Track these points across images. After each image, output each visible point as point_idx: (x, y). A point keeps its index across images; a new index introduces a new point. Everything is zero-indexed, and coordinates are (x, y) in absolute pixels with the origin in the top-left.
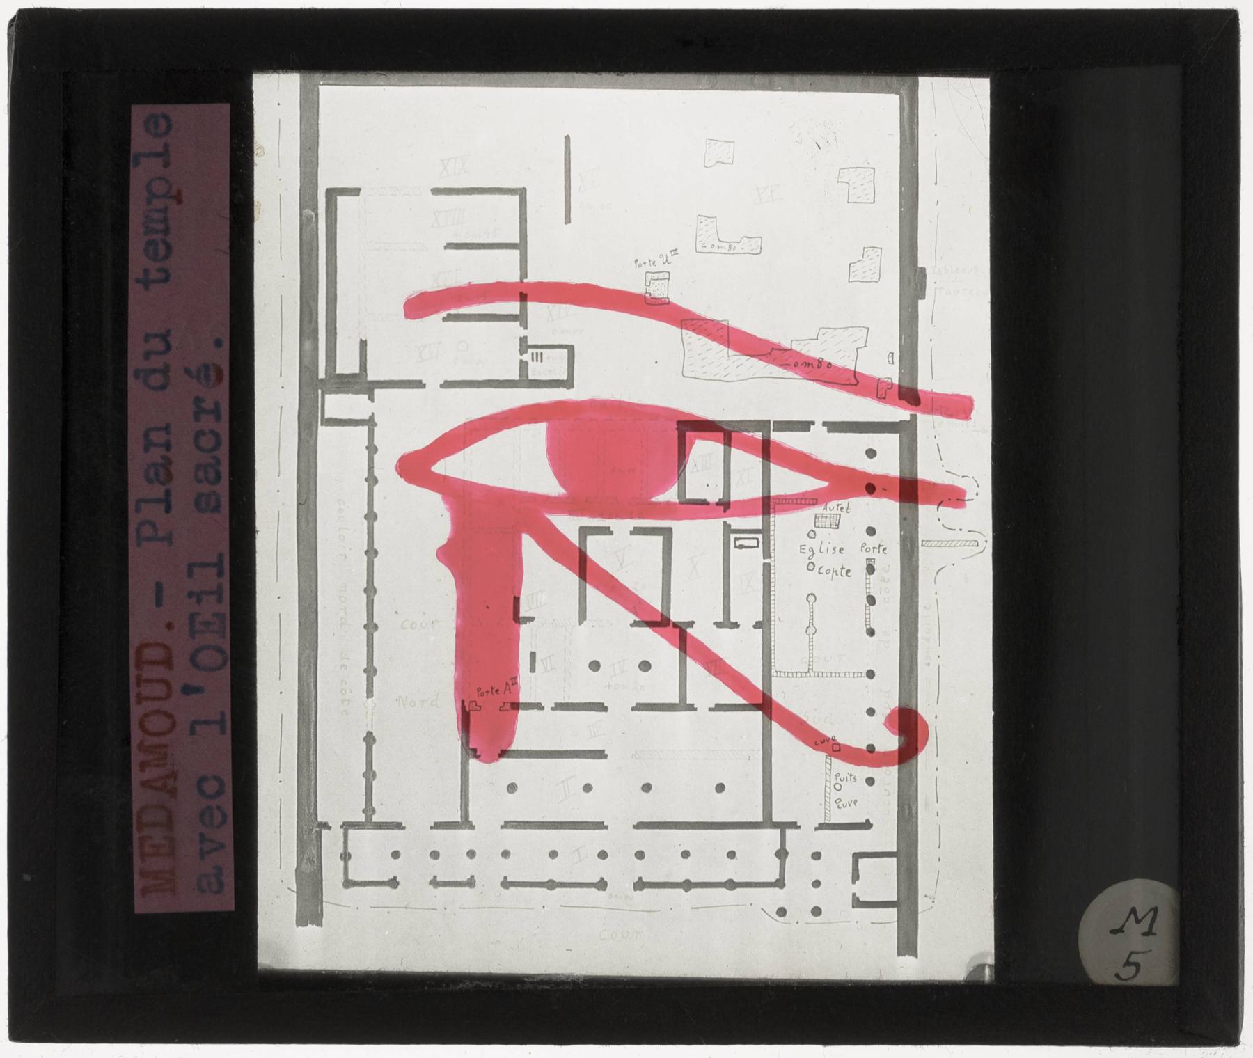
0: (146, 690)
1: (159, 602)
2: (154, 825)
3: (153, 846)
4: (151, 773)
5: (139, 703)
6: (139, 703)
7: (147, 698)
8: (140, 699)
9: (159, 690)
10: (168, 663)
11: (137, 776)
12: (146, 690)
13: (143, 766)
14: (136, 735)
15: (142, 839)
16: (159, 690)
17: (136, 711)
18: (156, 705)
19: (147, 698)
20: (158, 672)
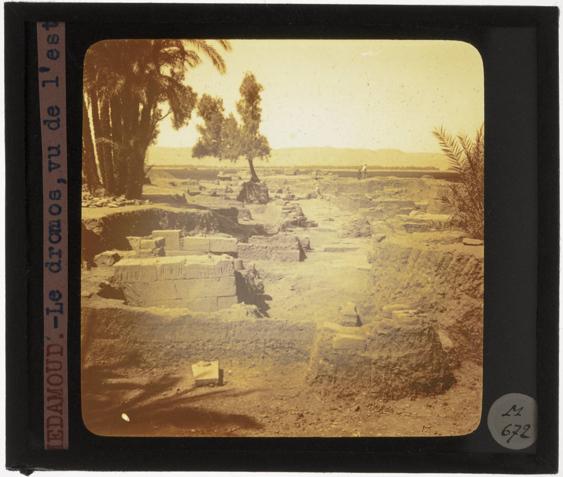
0: (51, 366)
1: (56, 326)
3: (52, 435)
4: (53, 402)
5: (47, 371)
6: (47, 371)
7: (51, 370)
8: (48, 370)
9: (57, 366)
11: (46, 404)
12: (51, 366)
13: (49, 399)
14: (46, 386)
15: (49, 432)
17: (46, 375)
18: (55, 372)
19: (51, 370)
20: (57, 357)
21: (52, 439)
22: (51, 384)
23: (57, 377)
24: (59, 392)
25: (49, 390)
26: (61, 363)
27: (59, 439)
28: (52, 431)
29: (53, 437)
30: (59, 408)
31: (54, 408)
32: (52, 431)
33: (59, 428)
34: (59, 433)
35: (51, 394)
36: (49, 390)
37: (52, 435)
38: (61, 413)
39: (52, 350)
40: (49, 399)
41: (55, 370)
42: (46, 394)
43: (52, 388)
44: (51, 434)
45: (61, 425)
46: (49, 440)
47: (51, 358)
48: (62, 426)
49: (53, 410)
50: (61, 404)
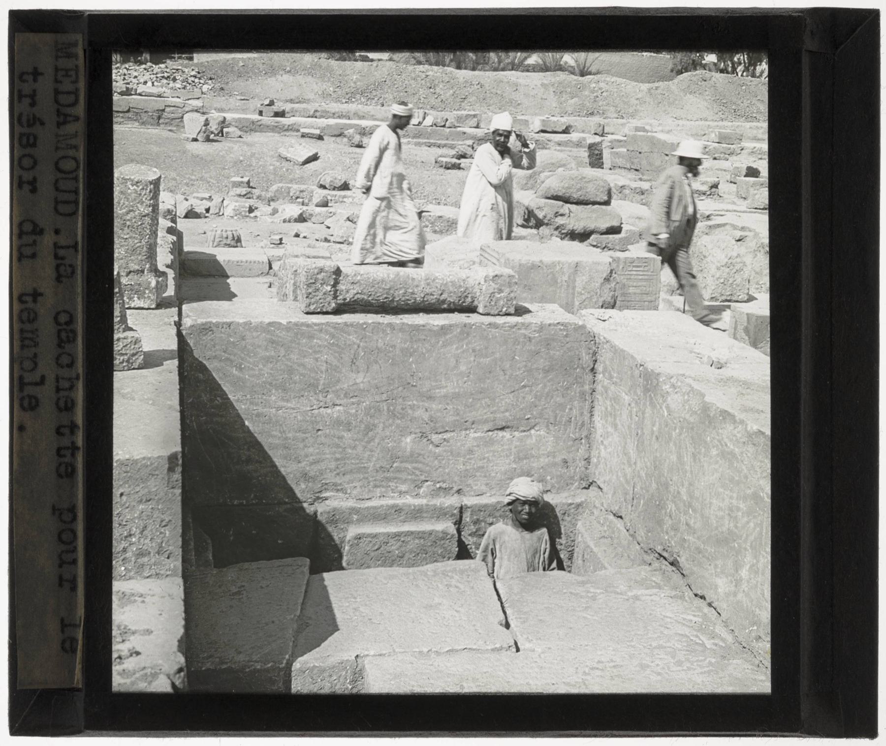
2: (69, 93)
3: (71, 76)
7: (73, 179)
13: (76, 135)
15: (76, 82)
18: (67, 176)
19: (73, 179)
25: (76, 147)
26: (57, 189)
27: (62, 70)
28: (73, 82)
30: (62, 119)
31: (69, 119)
32: (73, 82)
34: (59, 78)
36: (76, 147)
37: (71, 76)
38: (58, 111)
41: (66, 179)
43: (71, 153)
45: (57, 92)
47: (72, 197)
49: (70, 116)
50: (59, 125)
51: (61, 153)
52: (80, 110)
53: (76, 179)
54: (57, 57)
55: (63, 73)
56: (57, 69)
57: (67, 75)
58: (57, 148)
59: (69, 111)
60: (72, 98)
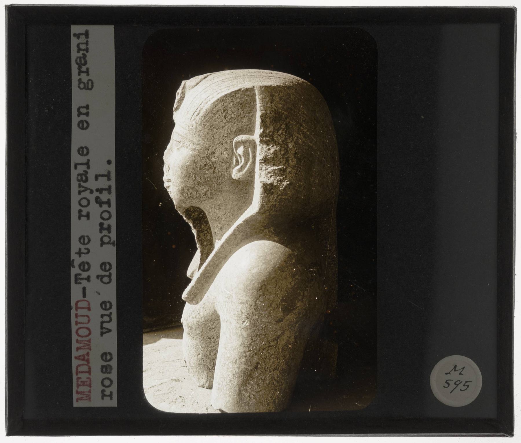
3: (81, 382)
7: (80, 323)
10: (89, 309)
12: (80, 319)
13: (78, 349)
15: (78, 379)
16: (85, 320)
19: (80, 323)
21: (80, 385)
22: (79, 335)
23: (85, 330)
24: (88, 343)
25: (77, 341)
27: (86, 385)
29: (82, 384)
33: (87, 375)
34: (87, 380)
35: (79, 345)
39: (80, 305)
40: (78, 349)
41: (84, 323)
42: (74, 345)
43: (80, 339)
44: (80, 380)
45: (89, 372)
46: (78, 386)
47: (80, 312)
48: (90, 374)
51: (87, 339)
52: (75, 363)
53: (77, 323)
54: (90, 392)
55: (86, 383)
56: (90, 385)
57: (83, 382)
58: (89, 341)
59: (82, 362)
60: (81, 369)
